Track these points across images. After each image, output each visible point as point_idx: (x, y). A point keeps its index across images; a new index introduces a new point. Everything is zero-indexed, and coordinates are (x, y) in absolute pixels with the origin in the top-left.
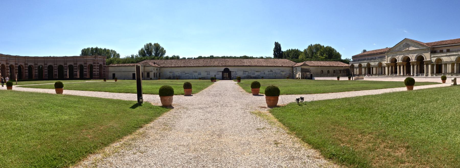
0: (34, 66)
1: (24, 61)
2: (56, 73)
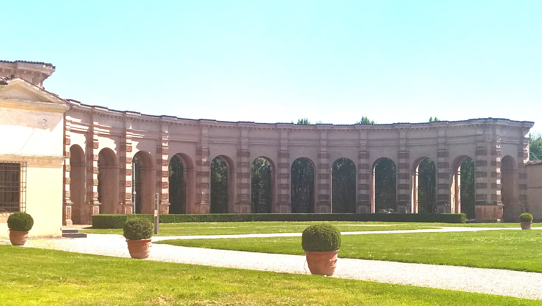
0: (235, 160)
2: (323, 192)
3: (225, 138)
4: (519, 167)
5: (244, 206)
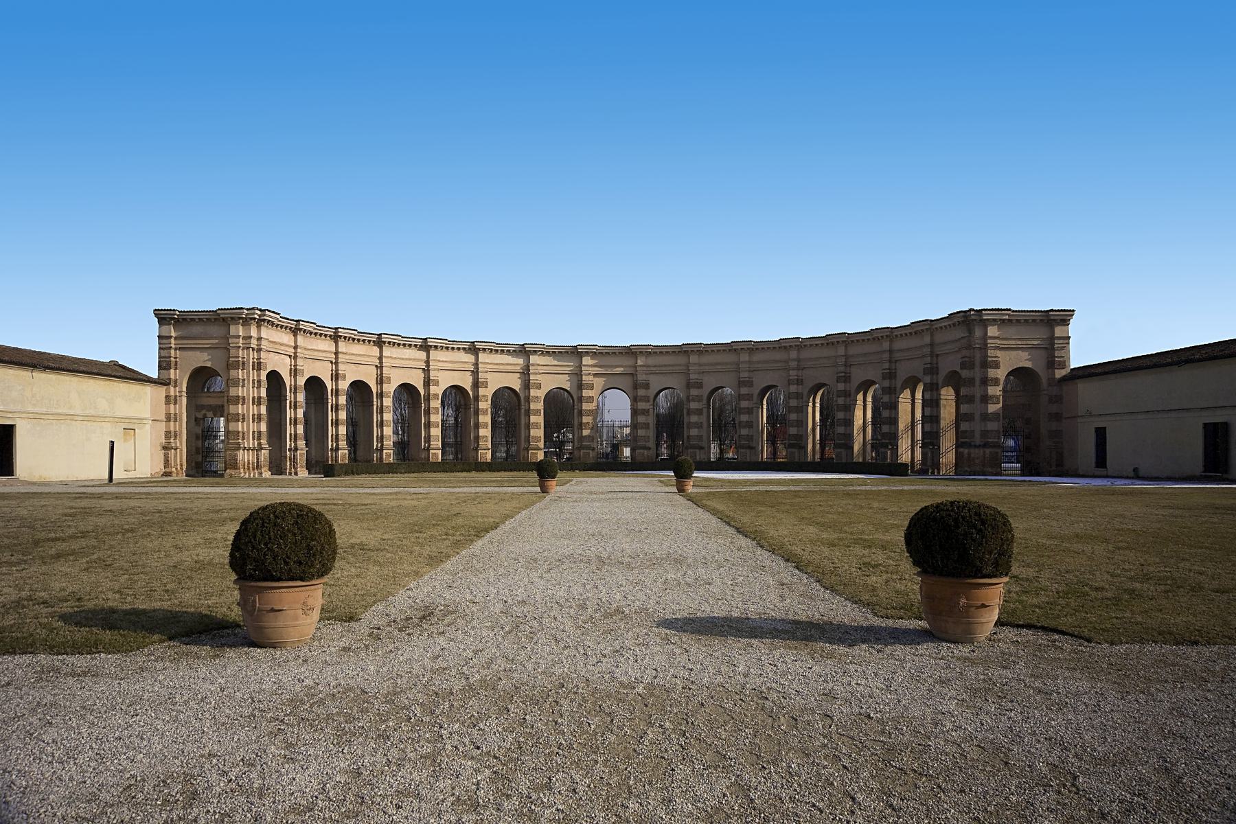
1: (629, 370)
3: (669, 366)
4: (1050, 385)
5: (692, 450)
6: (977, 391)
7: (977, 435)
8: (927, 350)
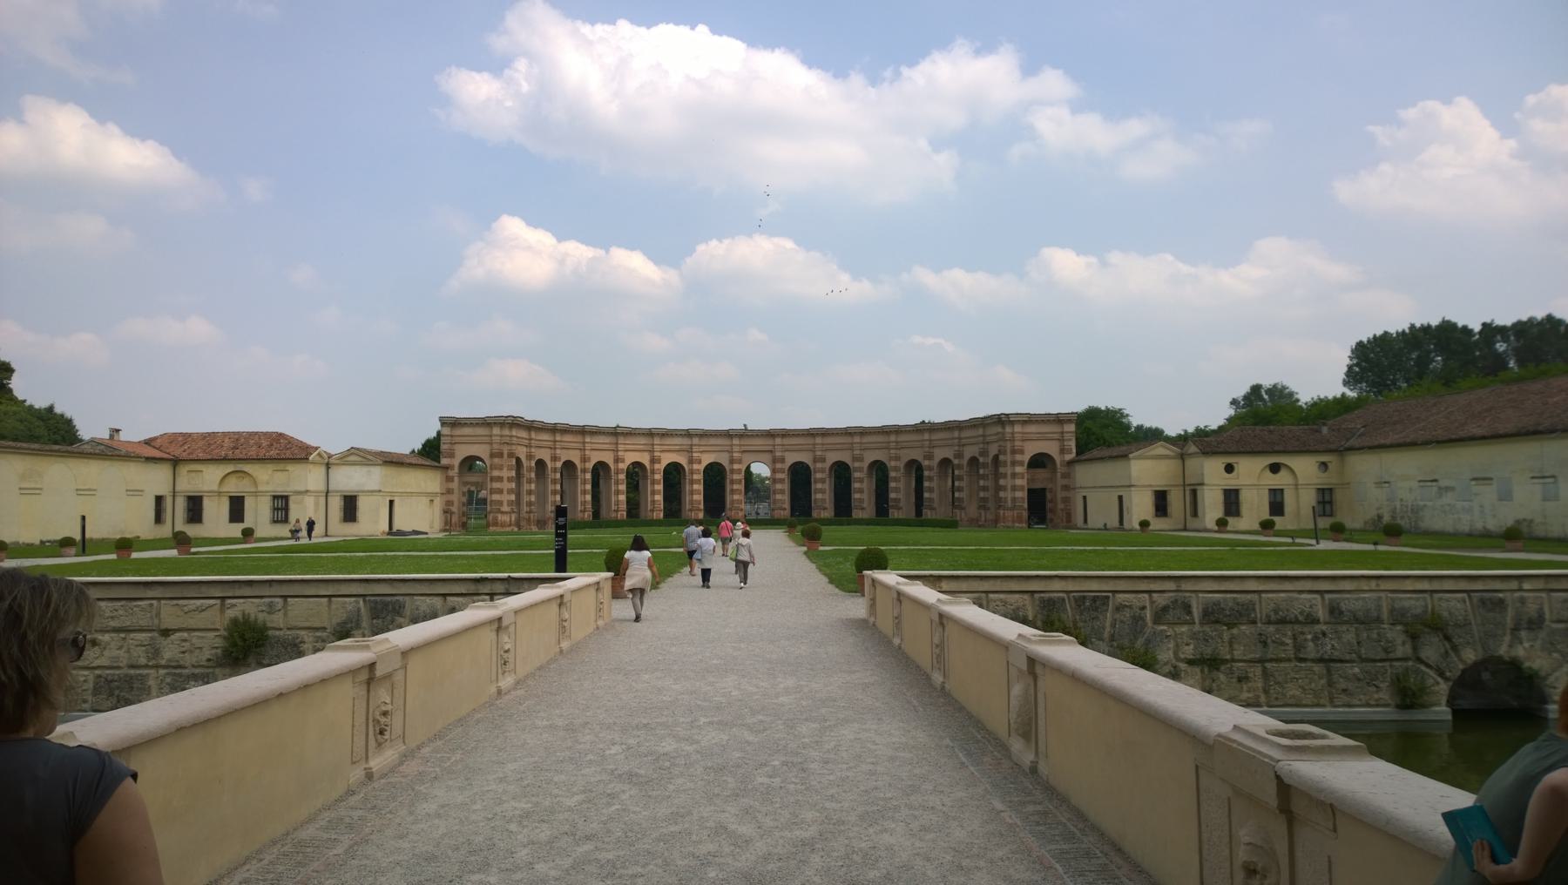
4: (1061, 465)
6: (1009, 470)
7: (1009, 499)
8: (981, 439)
